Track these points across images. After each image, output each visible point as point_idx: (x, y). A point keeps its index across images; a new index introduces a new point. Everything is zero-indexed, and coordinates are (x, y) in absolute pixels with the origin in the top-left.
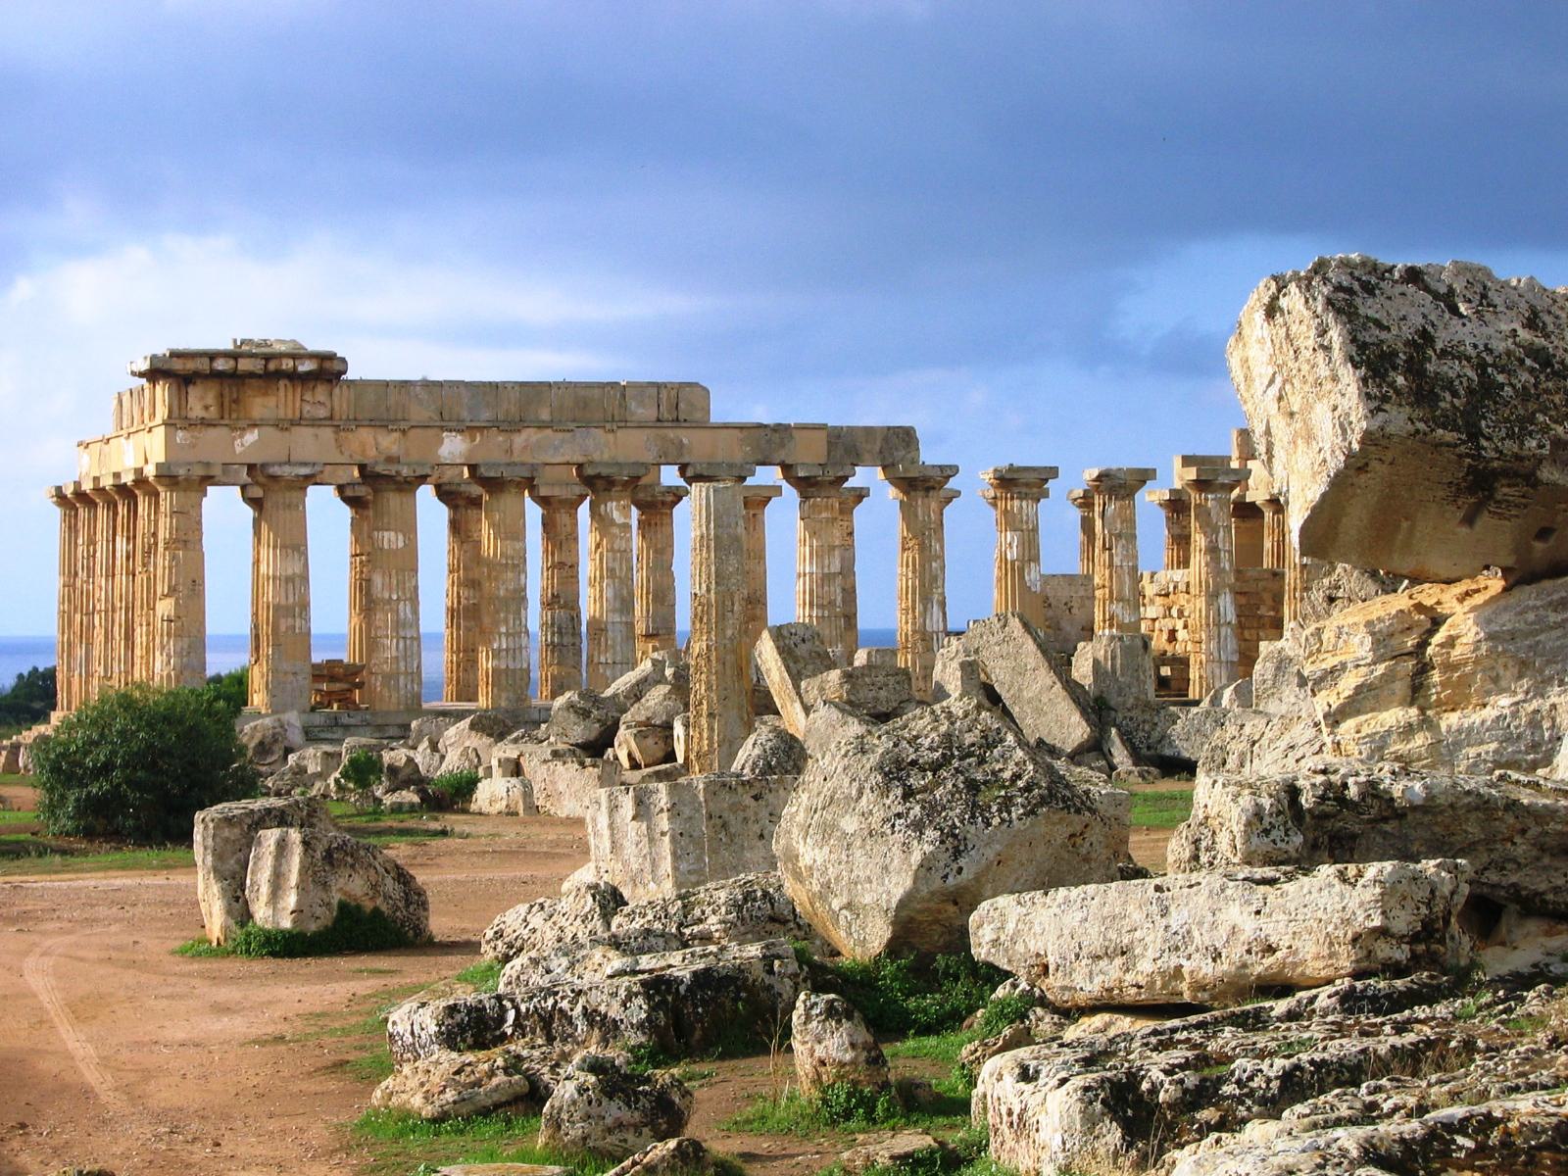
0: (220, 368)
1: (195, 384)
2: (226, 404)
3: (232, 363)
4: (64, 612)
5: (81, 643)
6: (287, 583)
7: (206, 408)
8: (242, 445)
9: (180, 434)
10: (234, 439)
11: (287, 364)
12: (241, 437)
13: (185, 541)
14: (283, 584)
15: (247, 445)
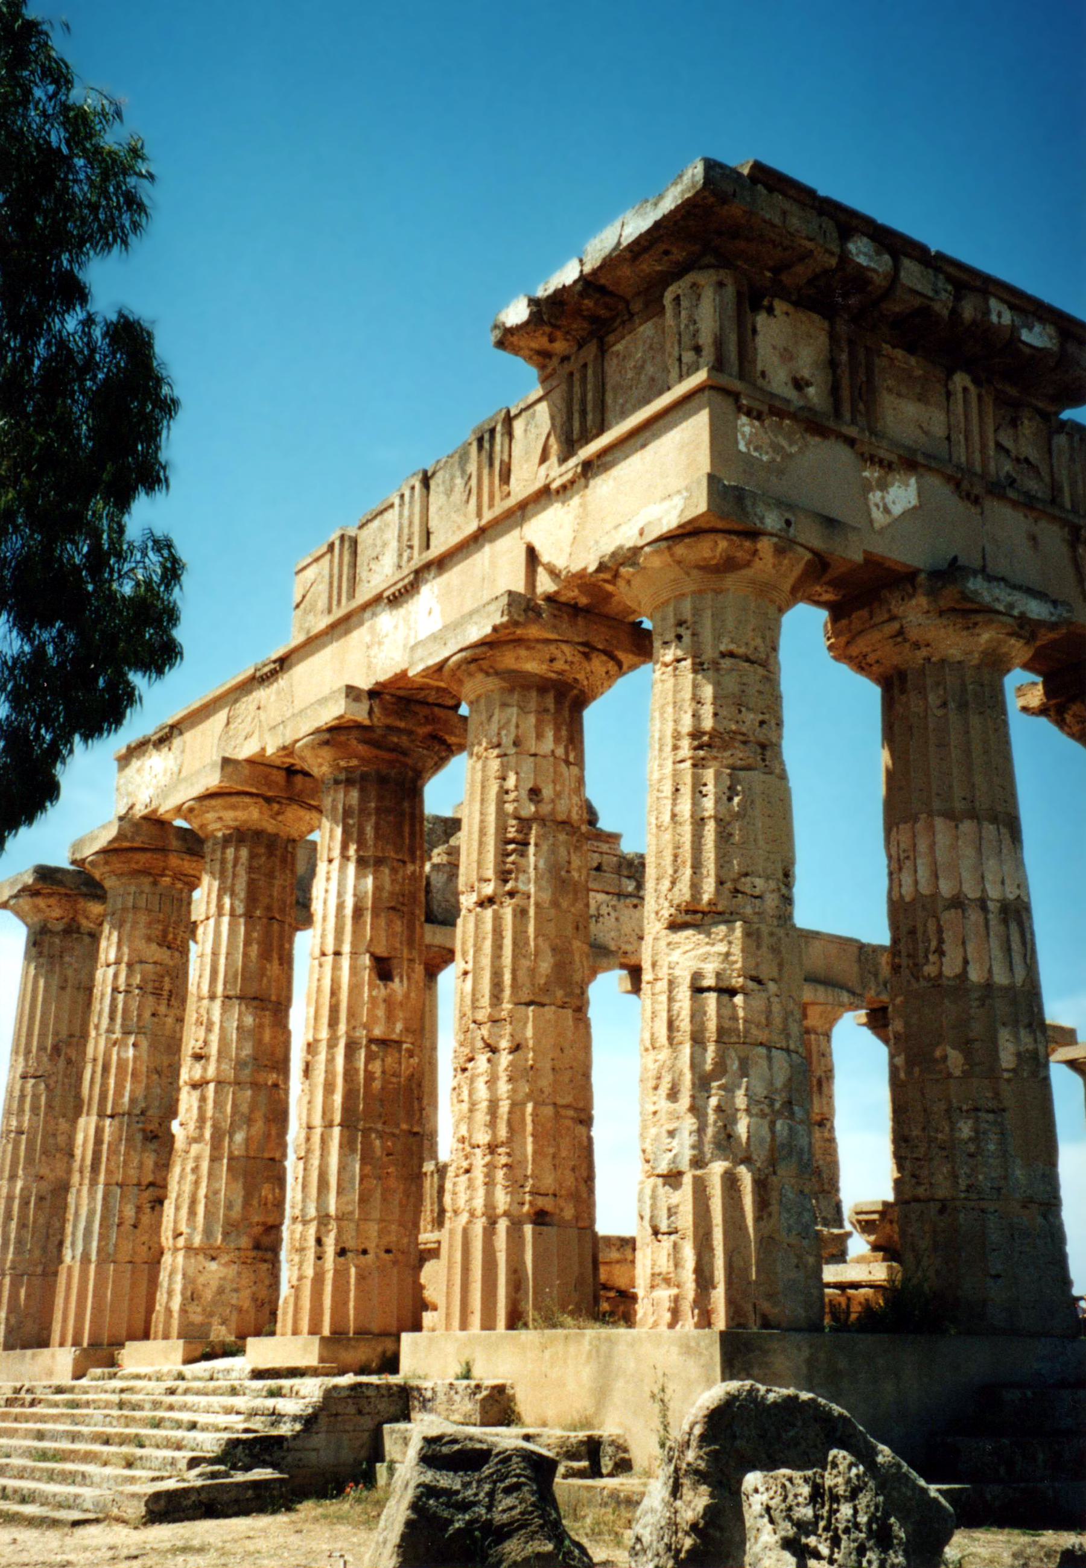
0: (862, 260)
1: (770, 311)
2: (845, 393)
3: (883, 264)
4: (20, 1132)
5: (93, 1183)
6: (1005, 922)
7: (799, 384)
8: (887, 511)
9: (746, 426)
10: (867, 488)
11: (1001, 315)
12: (883, 486)
13: (763, 747)
14: (994, 921)
15: (897, 510)
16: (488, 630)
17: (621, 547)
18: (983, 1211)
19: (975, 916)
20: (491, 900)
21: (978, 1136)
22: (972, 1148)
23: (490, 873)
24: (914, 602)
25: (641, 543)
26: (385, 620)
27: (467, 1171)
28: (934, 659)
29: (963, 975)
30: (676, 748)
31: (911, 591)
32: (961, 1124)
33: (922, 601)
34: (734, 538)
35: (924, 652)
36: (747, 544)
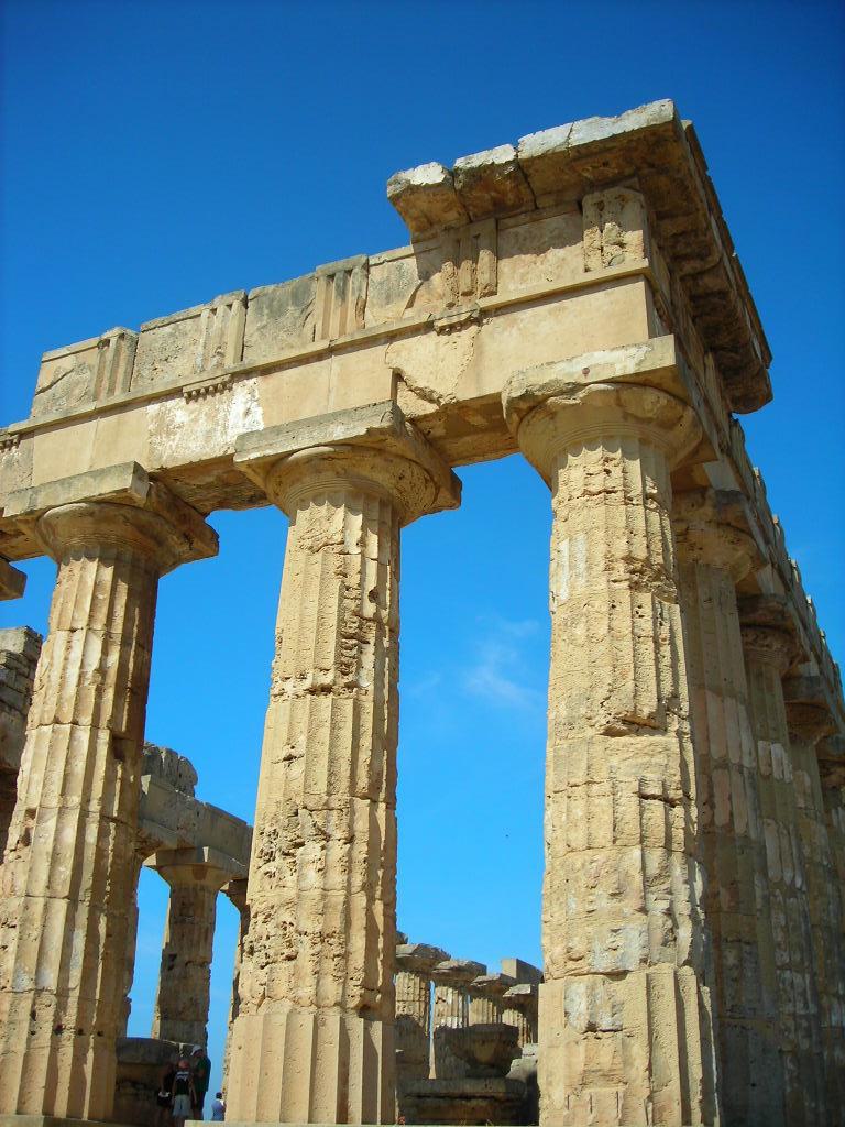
16: (363, 431)
17: (557, 381)
18: (743, 1028)
19: (736, 778)
20: (326, 690)
21: (740, 966)
22: (735, 974)
23: (330, 662)
24: (701, 511)
25: (583, 380)
26: (178, 410)
27: (290, 958)
28: (700, 562)
29: (730, 826)
30: (608, 569)
31: (700, 500)
32: (726, 953)
33: (708, 510)
34: (672, 399)
35: (696, 554)
36: (680, 408)
